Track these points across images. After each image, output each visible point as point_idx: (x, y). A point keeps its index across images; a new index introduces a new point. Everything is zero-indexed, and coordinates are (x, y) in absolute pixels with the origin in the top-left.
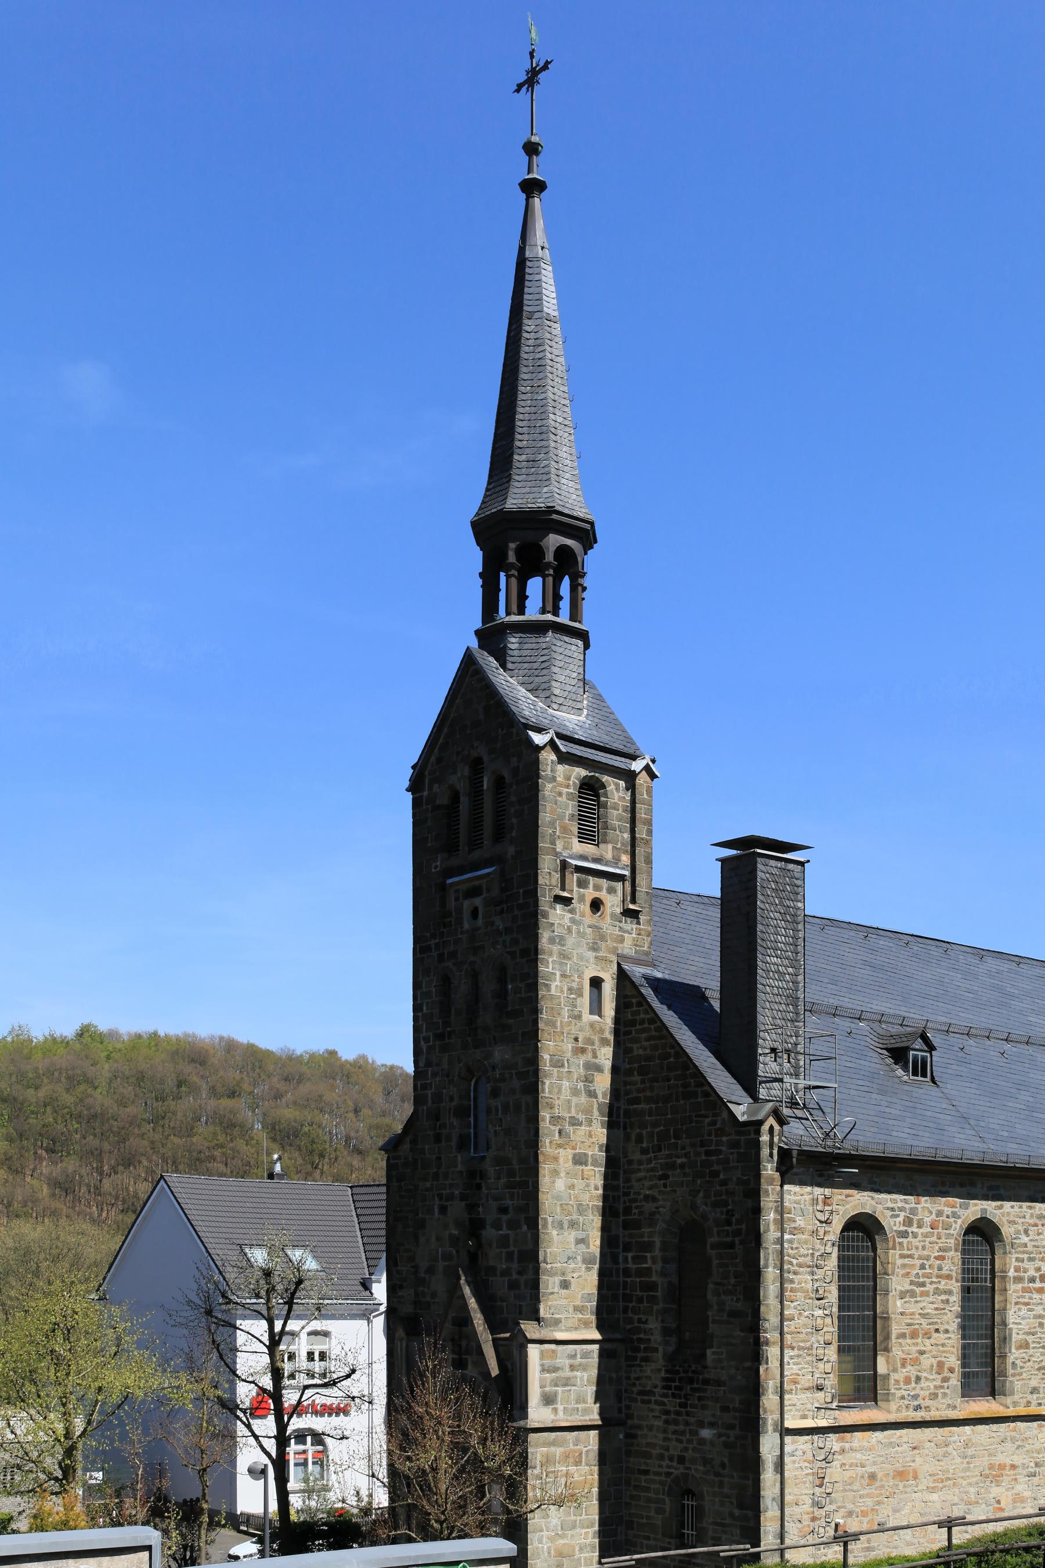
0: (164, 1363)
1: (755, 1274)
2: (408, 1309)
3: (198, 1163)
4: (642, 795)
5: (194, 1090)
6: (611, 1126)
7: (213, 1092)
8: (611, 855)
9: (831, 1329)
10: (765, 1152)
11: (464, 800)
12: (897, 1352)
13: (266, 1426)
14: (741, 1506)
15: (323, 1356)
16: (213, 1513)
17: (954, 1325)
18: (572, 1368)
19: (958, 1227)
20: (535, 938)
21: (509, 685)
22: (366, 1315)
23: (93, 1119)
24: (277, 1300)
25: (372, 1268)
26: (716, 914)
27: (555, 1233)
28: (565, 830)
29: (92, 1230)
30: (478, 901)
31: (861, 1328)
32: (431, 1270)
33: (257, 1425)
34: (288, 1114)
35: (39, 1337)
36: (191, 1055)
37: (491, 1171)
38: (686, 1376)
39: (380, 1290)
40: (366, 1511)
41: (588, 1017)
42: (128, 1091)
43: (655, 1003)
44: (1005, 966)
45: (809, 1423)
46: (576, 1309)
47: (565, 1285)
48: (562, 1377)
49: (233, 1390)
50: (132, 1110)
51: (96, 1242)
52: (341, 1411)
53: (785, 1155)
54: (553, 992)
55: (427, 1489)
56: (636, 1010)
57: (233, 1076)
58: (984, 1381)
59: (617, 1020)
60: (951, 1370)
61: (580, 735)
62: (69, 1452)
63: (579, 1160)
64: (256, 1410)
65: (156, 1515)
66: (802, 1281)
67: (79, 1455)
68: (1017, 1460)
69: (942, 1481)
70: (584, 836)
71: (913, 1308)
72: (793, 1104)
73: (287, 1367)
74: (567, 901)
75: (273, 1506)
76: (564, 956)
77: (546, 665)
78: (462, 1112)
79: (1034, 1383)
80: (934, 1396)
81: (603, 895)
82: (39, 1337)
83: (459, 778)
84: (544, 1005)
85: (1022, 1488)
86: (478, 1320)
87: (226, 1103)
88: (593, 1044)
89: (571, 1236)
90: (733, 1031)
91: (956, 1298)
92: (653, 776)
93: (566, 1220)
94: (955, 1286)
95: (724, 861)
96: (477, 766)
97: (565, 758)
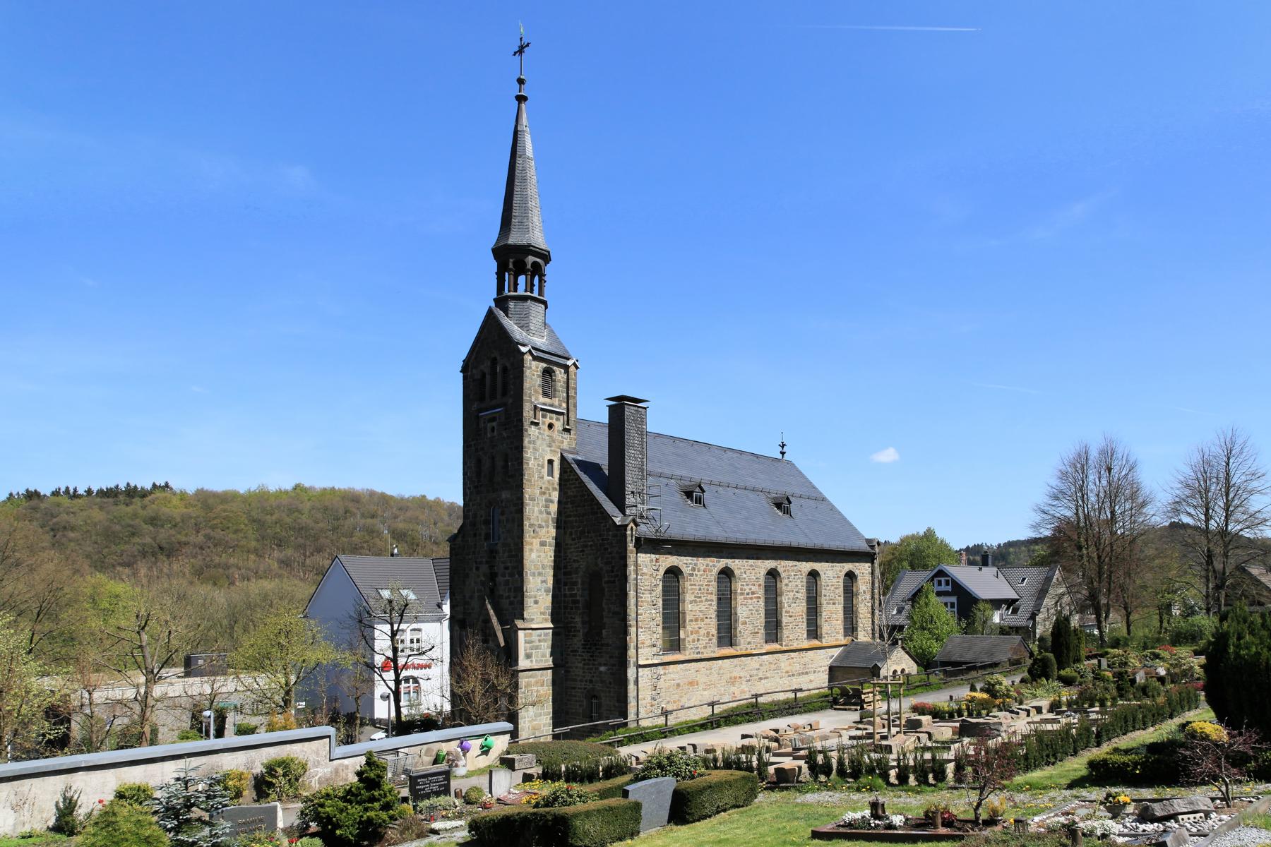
0: (337, 647)
1: (624, 595)
2: (461, 616)
3: (355, 550)
4: (572, 376)
5: (354, 515)
6: (558, 528)
7: (363, 516)
8: (558, 403)
9: (659, 619)
10: (629, 539)
11: (488, 377)
12: (689, 628)
13: (390, 675)
14: (619, 701)
15: (418, 641)
16: (361, 719)
17: (714, 616)
19: (715, 571)
20: (522, 441)
21: (510, 324)
22: (439, 620)
23: (301, 530)
24: (395, 615)
25: (442, 598)
26: (606, 431)
28: (536, 391)
29: (301, 584)
30: (494, 424)
31: (673, 618)
32: (471, 597)
33: (384, 675)
34: (401, 526)
35: (272, 637)
36: (353, 498)
37: (500, 548)
38: (593, 642)
39: (446, 608)
40: (440, 713)
41: (547, 478)
42: (319, 516)
43: (579, 472)
44: (735, 455)
45: (650, 662)
47: (536, 602)
48: (535, 645)
49: (373, 658)
50: (321, 525)
51: (303, 590)
52: (429, 667)
53: (638, 540)
55: (470, 701)
56: (570, 475)
57: (373, 508)
58: (727, 640)
59: (560, 479)
61: (543, 348)
62: (287, 693)
63: (543, 544)
64: (385, 668)
65: (333, 721)
66: (646, 597)
67: (293, 694)
68: (742, 674)
69: (708, 686)
70: (545, 394)
71: (696, 608)
72: (642, 517)
73: (400, 646)
74: (536, 424)
75: (393, 714)
76: (535, 449)
77: (527, 316)
78: (487, 522)
81: (554, 421)
82: (272, 637)
83: (486, 366)
84: (526, 472)
85: (744, 687)
86: (494, 620)
87: (369, 521)
89: (539, 579)
90: (614, 484)
91: (715, 603)
92: (577, 368)
94: (715, 598)
95: (610, 407)
96: (494, 362)
97: (535, 358)
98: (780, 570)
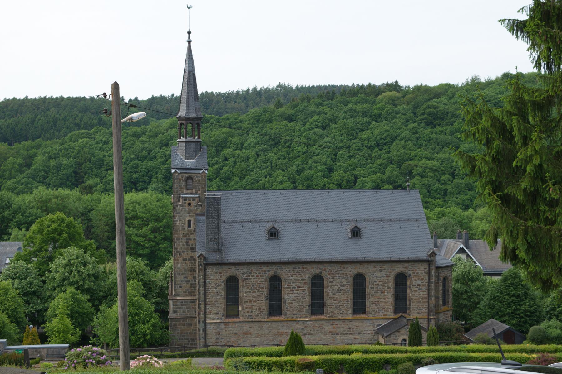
18: (182, 305)
46: (184, 292)
47: (181, 287)
60: (264, 309)
63: (184, 260)
71: (249, 295)
79: (295, 312)
80: (257, 316)
93: (181, 273)
98: (324, 274)
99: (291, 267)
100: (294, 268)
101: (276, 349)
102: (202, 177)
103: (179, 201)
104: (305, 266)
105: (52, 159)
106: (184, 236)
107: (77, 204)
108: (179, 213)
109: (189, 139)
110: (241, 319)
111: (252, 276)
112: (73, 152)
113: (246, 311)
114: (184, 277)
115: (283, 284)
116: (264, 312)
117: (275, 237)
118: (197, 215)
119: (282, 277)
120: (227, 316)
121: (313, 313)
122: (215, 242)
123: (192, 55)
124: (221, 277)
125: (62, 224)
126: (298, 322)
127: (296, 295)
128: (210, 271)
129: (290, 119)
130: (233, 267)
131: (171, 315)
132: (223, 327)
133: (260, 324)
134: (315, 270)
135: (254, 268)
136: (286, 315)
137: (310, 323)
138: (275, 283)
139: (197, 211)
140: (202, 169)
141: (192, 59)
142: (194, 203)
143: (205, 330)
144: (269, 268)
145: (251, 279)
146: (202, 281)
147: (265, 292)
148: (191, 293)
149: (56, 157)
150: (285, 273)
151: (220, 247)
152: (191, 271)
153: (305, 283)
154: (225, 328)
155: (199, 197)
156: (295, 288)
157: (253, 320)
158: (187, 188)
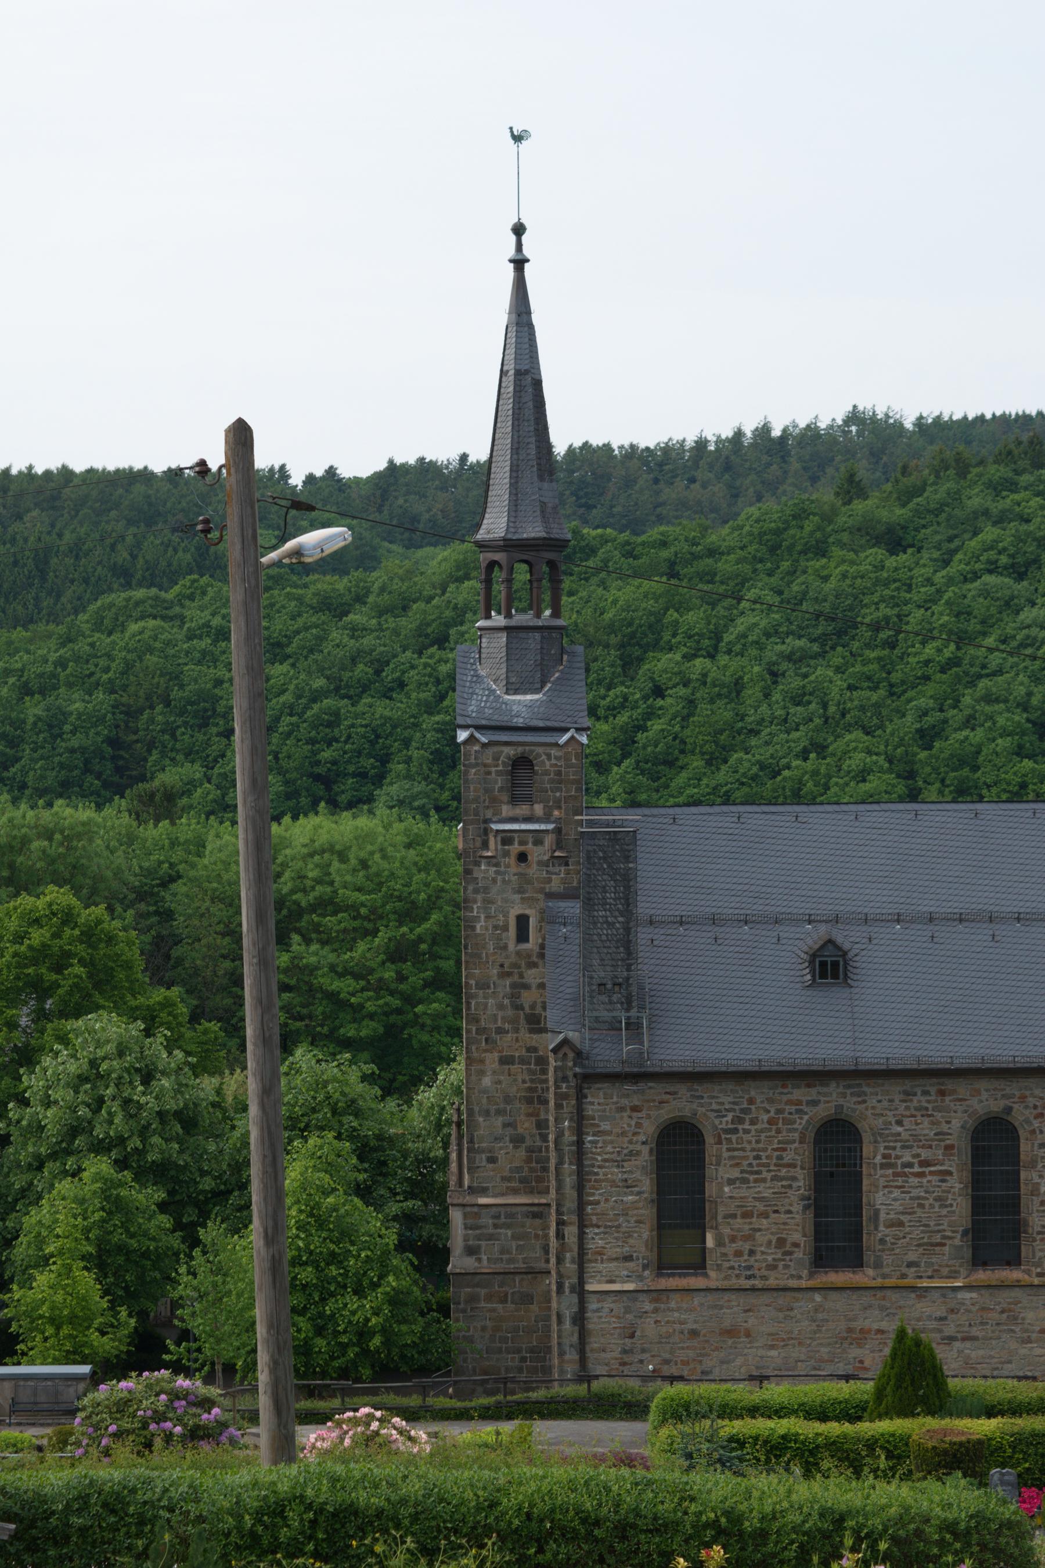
18: (495, 1226)
27: (481, 1119)
46: (503, 1179)
47: (492, 1160)
54: (478, 931)
60: (796, 1245)
71: (743, 1192)
79: (912, 1257)
80: (773, 1267)
88: (519, 967)
93: (493, 1108)
98: (1020, 1115)
99: (895, 1089)
100: (907, 1093)
101: (842, 1390)
102: (567, 757)
103: (485, 845)
104: (949, 1084)
105: (32, 694)
106: (504, 975)
107: (119, 858)
108: (486, 890)
109: (521, 619)
110: (714, 1278)
111: (753, 1122)
112: (107, 670)
113: (730, 1249)
114: (505, 1125)
115: (867, 1150)
116: (799, 1254)
117: (836, 976)
118: (550, 896)
119: (863, 1126)
120: (663, 1266)
121: (979, 1260)
122: (615, 998)
123: (529, 313)
124: (638, 1125)
125: (68, 932)
126: (922, 1292)
127: (915, 1193)
128: (599, 1102)
129: (895, 540)
130: (682, 1089)
131: (458, 1262)
132: (648, 1307)
133: (782, 1300)
134: (986, 1100)
135: (758, 1092)
136: (878, 1265)
137: (967, 1295)
138: (837, 1149)
139: (550, 880)
140: (566, 730)
141: (531, 326)
142: (537, 854)
143: (580, 1319)
144: (813, 1093)
145: (747, 1132)
146: (569, 1137)
147: (802, 1182)
148: (532, 1179)
149: (46, 687)
150: (875, 1112)
151: (633, 1013)
152: (529, 1101)
153: (949, 1148)
154: (656, 1310)
155: (558, 831)
156: (910, 1165)
157: (757, 1283)
158: (514, 800)
